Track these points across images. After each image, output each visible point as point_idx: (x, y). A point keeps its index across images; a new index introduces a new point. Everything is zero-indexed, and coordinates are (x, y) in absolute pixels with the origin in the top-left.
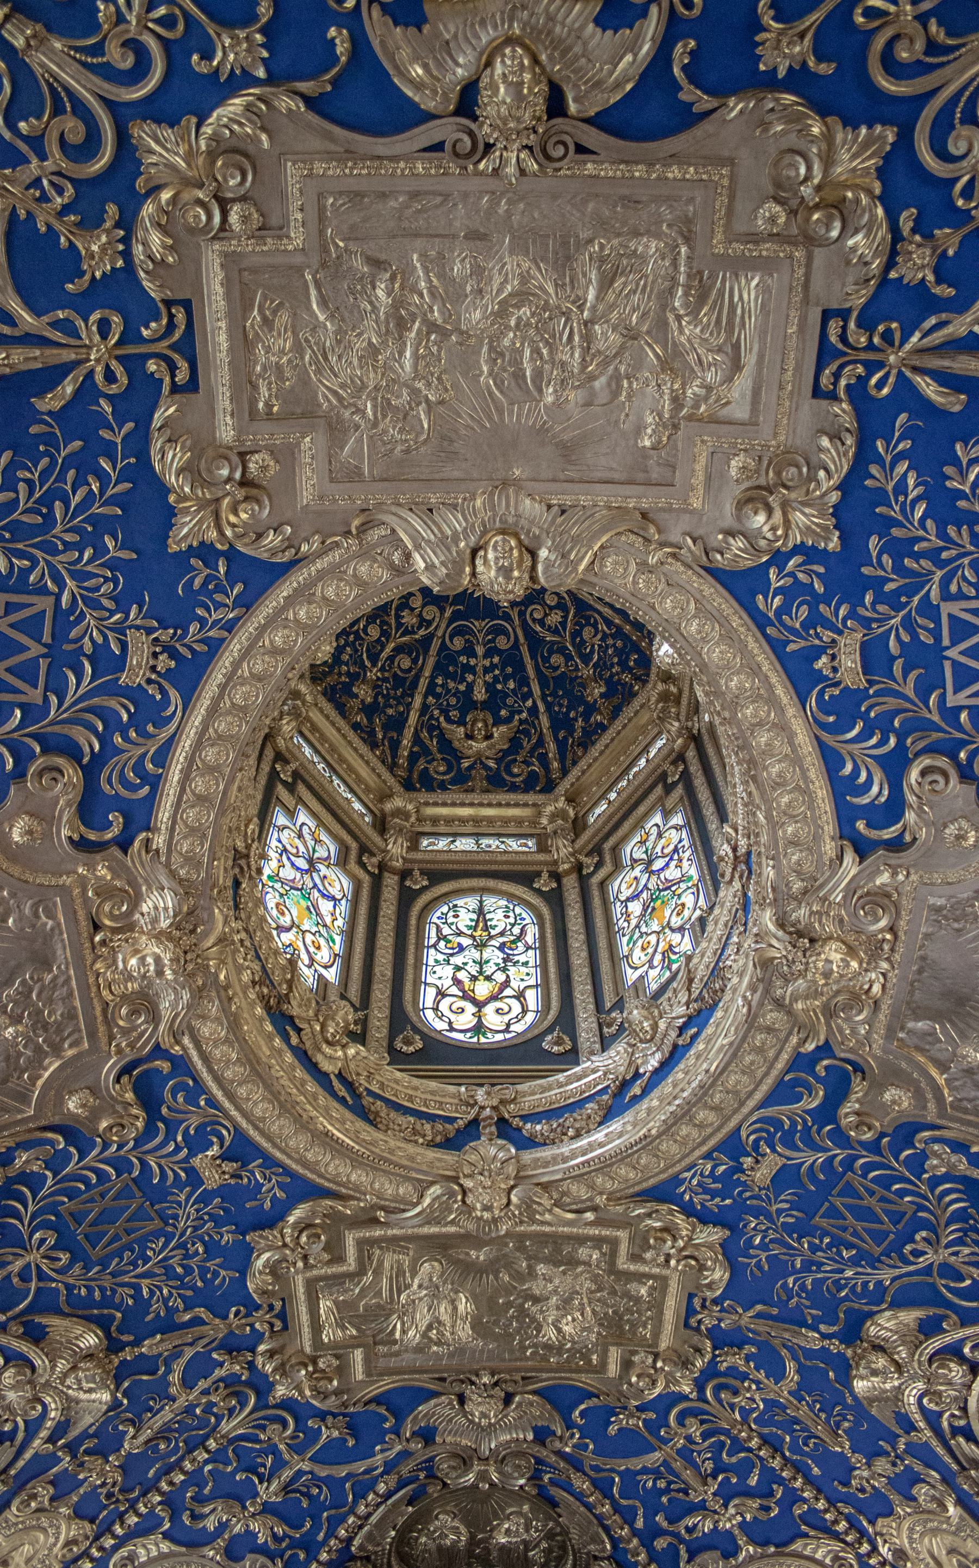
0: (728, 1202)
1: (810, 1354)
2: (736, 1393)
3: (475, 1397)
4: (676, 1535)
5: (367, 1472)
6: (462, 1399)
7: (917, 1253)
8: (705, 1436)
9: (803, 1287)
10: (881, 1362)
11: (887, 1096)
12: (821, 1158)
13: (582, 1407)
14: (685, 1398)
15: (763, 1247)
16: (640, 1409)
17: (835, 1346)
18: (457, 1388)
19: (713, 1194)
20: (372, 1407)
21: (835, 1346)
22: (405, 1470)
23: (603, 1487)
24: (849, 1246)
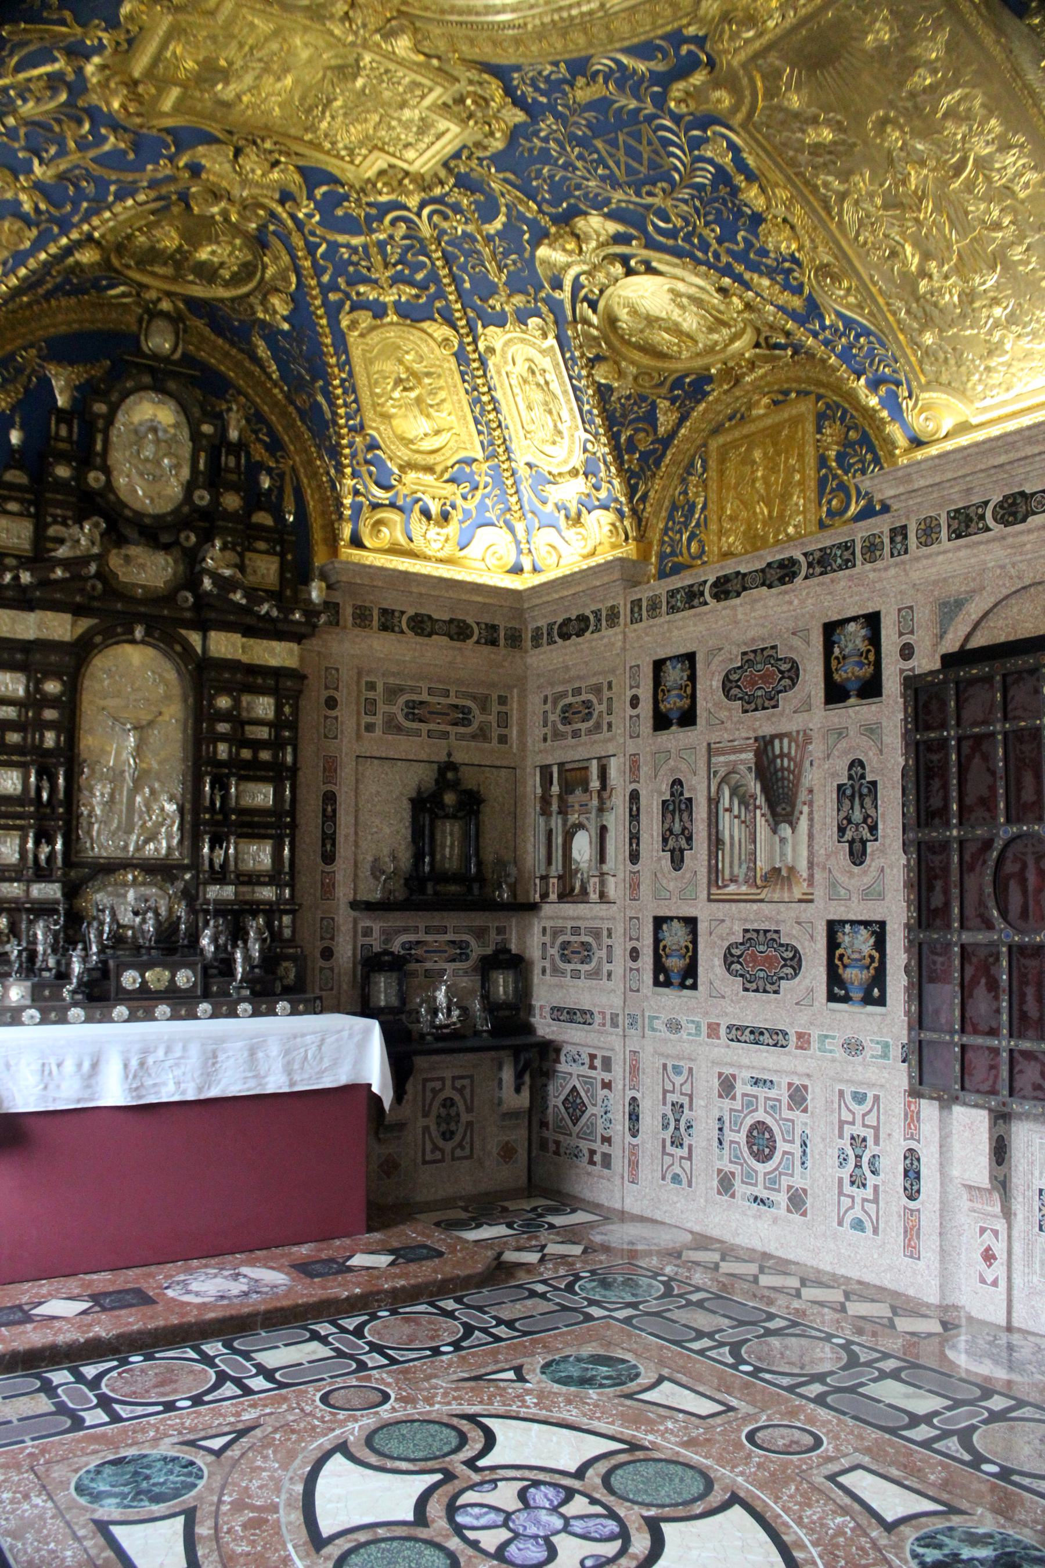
0: (544, 100)
1: (522, 218)
2: (446, 218)
3: (254, 157)
4: (348, 296)
5: (135, 182)
6: (238, 152)
7: (650, 194)
8: (404, 238)
9: (551, 177)
10: (571, 246)
11: (717, 94)
12: (633, 104)
13: (324, 189)
14: (408, 209)
15: (546, 140)
16: (369, 204)
17: (544, 221)
18: (242, 143)
19: (537, 89)
20: (164, 135)
21: (544, 221)
22: (164, 191)
23: (311, 249)
24: (606, 167)
